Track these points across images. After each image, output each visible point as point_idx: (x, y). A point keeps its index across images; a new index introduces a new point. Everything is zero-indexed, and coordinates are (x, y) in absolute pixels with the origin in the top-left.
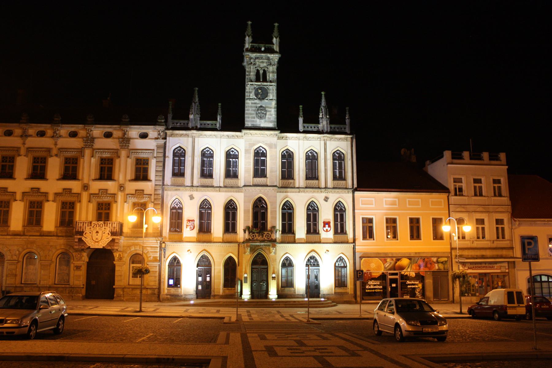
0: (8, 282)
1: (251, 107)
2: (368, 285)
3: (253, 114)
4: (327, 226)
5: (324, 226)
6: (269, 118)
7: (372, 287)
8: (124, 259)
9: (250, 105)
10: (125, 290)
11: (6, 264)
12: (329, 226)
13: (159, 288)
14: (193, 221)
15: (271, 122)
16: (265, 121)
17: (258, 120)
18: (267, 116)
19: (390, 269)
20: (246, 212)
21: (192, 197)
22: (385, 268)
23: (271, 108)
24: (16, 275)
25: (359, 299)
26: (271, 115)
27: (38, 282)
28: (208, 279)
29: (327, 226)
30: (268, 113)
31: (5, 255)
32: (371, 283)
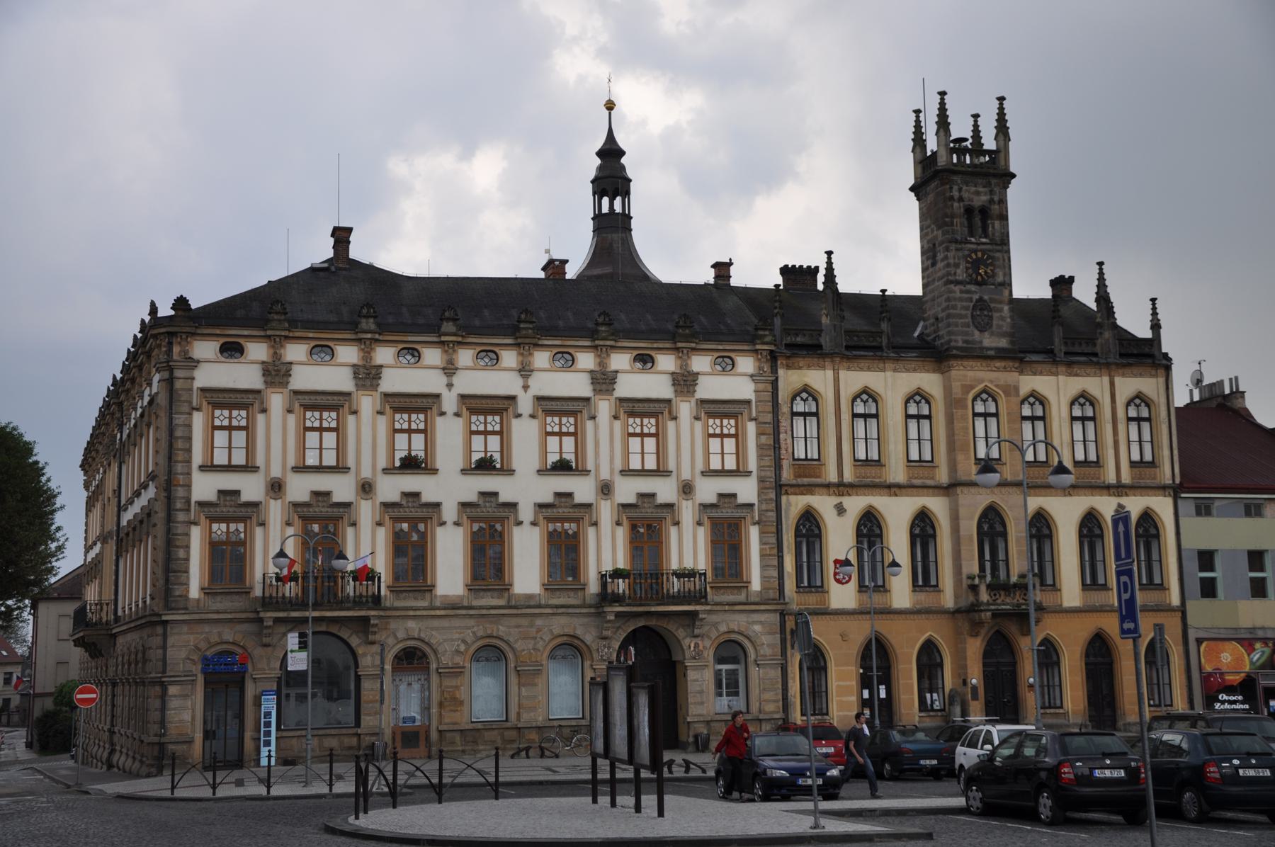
0: (446, 720)
1: (961, 299)
2: (1219, 701)
3: (966, 316)
6: (999, 327)
7: (1227, 706)
9: (958, 295)
10: (713, 724)
11: (434, 679)
15: (1003, 335)
16: (992, 334)
17: (977, 333)
18: (995, 322)
21: (840, 510)
23: (1001, 302)
26: (1003, 319)
28: (883, 695)
30: (996, 315)
32: (1225, 697)
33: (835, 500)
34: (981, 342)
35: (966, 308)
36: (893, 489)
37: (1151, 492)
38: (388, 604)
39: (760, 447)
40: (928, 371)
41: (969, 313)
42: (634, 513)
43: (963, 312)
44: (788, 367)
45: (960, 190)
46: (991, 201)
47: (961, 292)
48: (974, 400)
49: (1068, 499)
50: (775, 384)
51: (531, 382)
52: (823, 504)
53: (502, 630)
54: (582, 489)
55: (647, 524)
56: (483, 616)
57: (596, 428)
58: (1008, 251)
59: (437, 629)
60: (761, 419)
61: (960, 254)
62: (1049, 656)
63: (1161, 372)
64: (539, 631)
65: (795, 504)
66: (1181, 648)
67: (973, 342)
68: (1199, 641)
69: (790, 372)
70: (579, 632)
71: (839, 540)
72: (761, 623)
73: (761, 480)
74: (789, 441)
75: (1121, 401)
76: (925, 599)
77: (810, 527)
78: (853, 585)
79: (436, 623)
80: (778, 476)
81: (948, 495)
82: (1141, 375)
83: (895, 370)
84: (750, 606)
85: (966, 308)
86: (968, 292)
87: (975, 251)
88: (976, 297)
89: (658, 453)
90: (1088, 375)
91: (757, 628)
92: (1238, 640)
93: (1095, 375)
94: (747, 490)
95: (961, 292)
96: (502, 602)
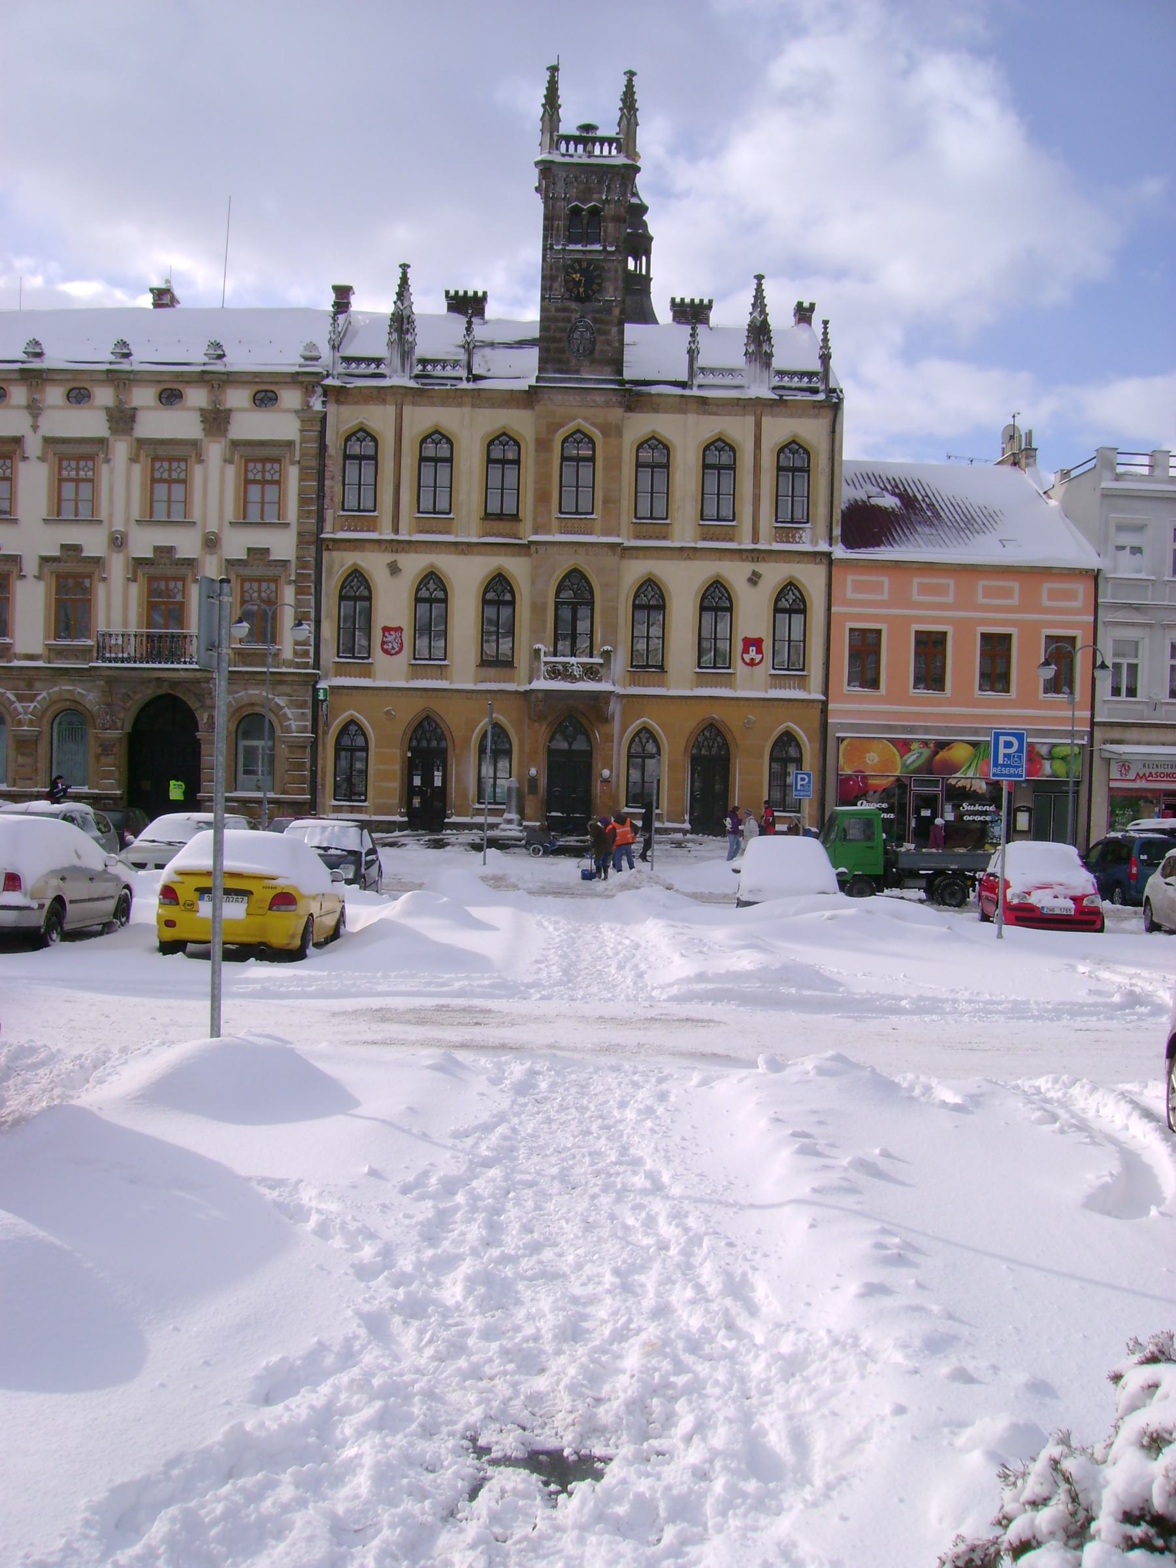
4: (753, 649)
12: (759, 651)
14: (400, 629)
19: (917, 770)
20: (537, 609)
21: (394, 569)
22: (904, 765)
29: (753, 649)
33: (389, 558)
39: (302, 492)
42: (54, 566)
43: (558, 335)
48: (565, 441)
49: (689, 563)
51: (41, 421)
52: (374, 564)
55: (162, 577)
57: (112, 471)
65: (339, 563)
66: (817, 746)
69: (343, 408)
71: (393, 605)
73: (300, 534)
74: (338, 489)
77: (357, 589)
78: (404, 657)
80: (320, 529)
81: (529, 555)
83: (473, 406)
85: (563, 330)
86: (565, 310)
89: (152, 502)
94: (283, 545)
95: (558, 310)
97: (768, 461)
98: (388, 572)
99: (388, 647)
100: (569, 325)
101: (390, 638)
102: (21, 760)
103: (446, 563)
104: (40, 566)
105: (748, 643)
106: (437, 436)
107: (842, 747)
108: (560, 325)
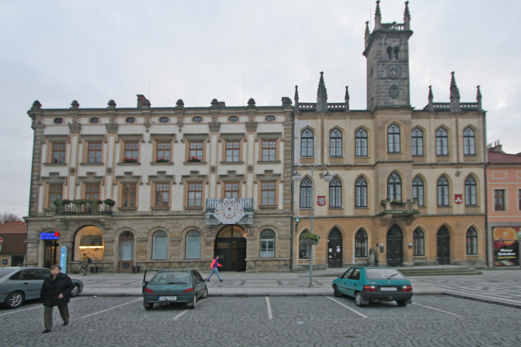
0: (139, 259)
1: (384, 85)
3: (386, 92)
5: (456, 199)
7: (504, 254)
8: (255, 234)
9: (382, 83)
10: (257, 262)
12: (461, 199)
13: (291, 261)
14: (324, 197)
16: (399, 99)
23: (404, 86)
24: (146, 252)
25: (491, 266)
27: (169, 258)
28: (338, 250)
30: (401, 91)
31: (135, 234)
34: (393, 103)
35: (387, 89)
36: (348, 167)
37: (474, 166)
38: (117, 214)
40: (367, 119)
41: (388, 91)
43: (385, 91)
44: (300, 119)
45: (385, 40)
46: (401, 44)
47: (384, 82)
48: (388, 127)
49: (433, 170)
50: (293, 125)
53: (163, 224)
54: (203, 170)
56: (156, 219)
58: (408, 65)
59: (137, 224)
60: (286, 140)
61: (384, 66)
62: (418, 233)
63: (481, 116)
64: (180, 225)
66: (484, 231)
67: (389, 103)
68: (493, 228)
70: (197, 225)
72: (281, 221)
73: (285, 164)
75: (461, 127)
76: (361, 212)
78: (326, 206)
79: (136, 222)
81: (374, 169)
82: (471, 118)
83: (351, 119)
84: (278, 216)
85: (387, 89)
86: (387, 82)
87: (392, 65)
88: (391, 84)
90: (445, 118)
91: (280, 224)
92: (513, 227)
93: (448, 118)
94: (278, 169)
95: (384, 82)
96: (167, 214)
97: (461, 133)
98: (319, 177)
99: (320, 203)
100: (389, 87)
101: (321, 200)
102: (173, 248)
103: (340, 173)
104: (182, 179)
105: (457, 196)
106: (337, 129)
107: (495, 230)
108: (386, 87)
